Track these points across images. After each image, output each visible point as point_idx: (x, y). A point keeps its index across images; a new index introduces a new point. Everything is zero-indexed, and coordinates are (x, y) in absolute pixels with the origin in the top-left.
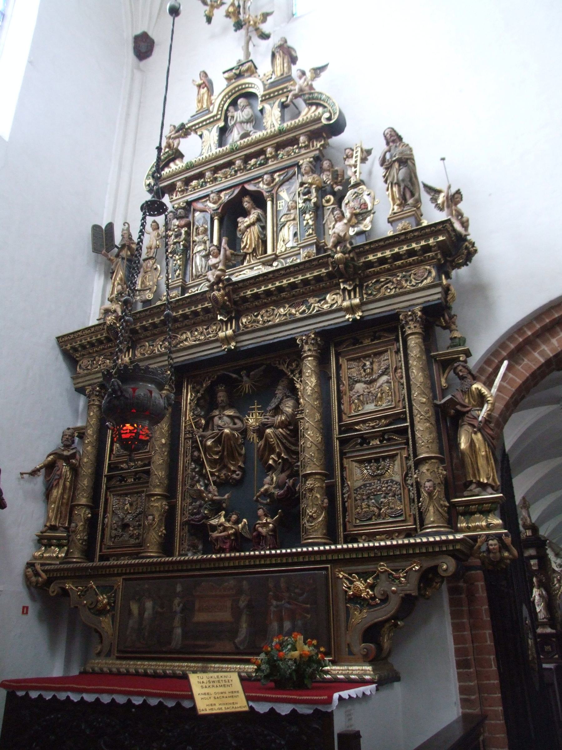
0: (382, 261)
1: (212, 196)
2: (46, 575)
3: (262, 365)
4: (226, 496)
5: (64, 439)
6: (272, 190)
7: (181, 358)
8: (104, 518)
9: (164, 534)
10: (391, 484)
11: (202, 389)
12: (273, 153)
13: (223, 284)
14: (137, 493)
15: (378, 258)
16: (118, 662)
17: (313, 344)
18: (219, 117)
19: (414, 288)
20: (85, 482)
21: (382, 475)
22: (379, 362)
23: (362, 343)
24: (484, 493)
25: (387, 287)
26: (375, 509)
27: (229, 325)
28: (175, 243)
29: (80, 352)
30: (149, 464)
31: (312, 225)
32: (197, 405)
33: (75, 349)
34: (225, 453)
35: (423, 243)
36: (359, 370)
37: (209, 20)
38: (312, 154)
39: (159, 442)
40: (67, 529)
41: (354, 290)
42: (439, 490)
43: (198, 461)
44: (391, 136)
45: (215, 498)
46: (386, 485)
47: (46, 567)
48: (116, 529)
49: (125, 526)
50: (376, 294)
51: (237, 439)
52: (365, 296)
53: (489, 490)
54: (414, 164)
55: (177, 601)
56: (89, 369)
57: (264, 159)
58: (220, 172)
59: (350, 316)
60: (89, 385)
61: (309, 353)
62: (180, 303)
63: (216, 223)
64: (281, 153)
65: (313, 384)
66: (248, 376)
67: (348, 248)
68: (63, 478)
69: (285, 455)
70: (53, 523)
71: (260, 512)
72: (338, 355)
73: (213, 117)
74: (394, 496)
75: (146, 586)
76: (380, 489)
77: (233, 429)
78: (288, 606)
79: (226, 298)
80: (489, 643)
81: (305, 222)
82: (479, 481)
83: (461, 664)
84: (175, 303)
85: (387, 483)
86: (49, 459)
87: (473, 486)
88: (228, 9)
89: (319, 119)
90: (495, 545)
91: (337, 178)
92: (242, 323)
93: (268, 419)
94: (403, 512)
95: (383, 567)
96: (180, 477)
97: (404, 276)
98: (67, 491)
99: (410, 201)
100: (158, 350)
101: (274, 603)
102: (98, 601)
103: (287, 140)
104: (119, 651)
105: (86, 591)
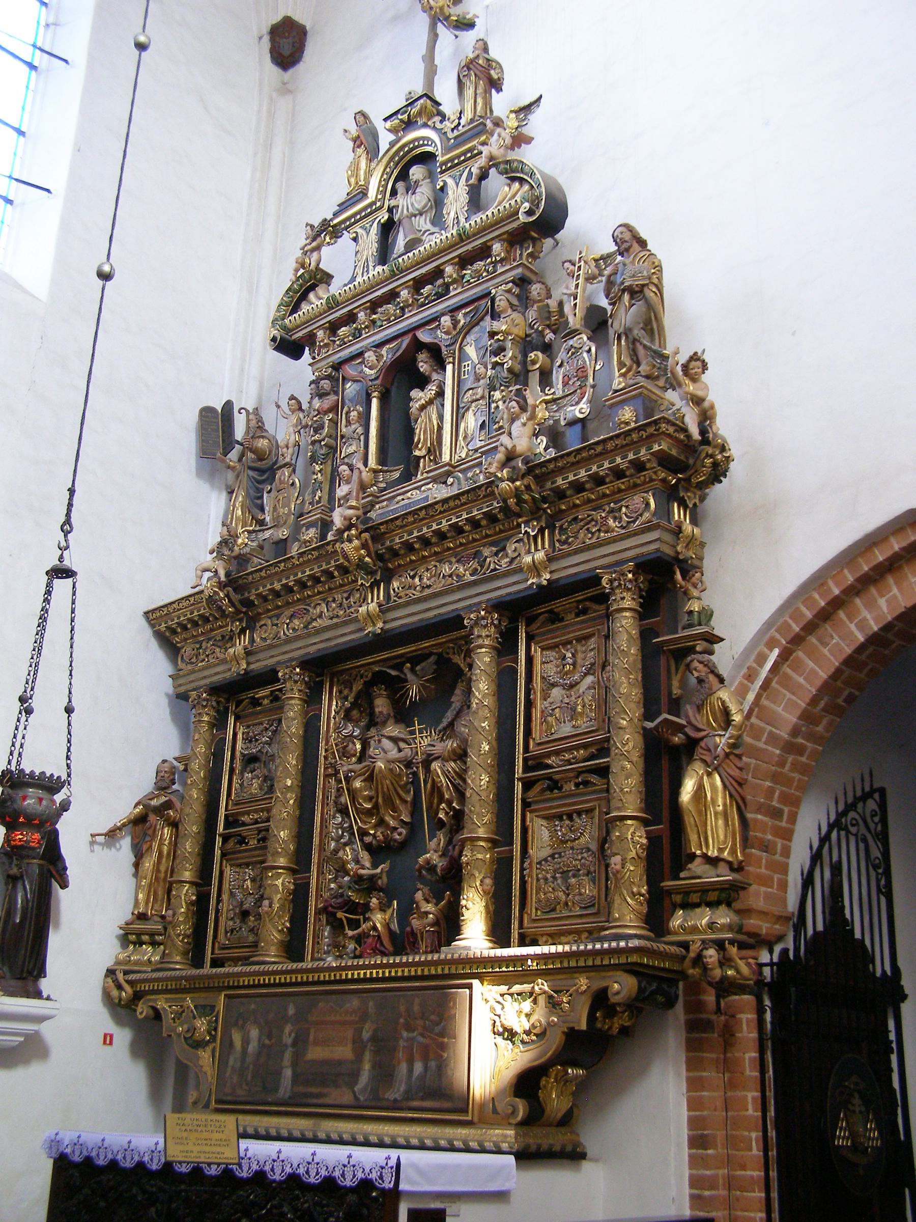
2: (132, 987)
3: (431, 654)
4: (379, 870)
6: (453, 344)
7: (314, 646)
9: (287, 928)
11: (353, 695)
12: (455, 276)
13: (357, 530)
15: (569, 483)
19: (623, 531)
20: (189, 846)
23: (562, 620)
30: (268, 820)
32: (348, 717)
33: (174, 632)
34: (380, 800)
35: (631, 456)
38: (509, 276)
41: (541, 531)
42: (632, 868)
45: (362, 872)
47: (132, 977)
48: (232, 919)
51: (400, 776)
52: (557, 545)
53: (723, 868)
55: (288, 1029)
60: (194, 690)
63: (375, 403)
66: (412, 670)
67: (520, 469)
72: (530, 638)
75: (253, 1006)
78: (421, 1039)
80: (750, 1112)
81: (493, 405)
83: (698, 1141)
87: (698, 861)
91: (549, 318)
92: (394, 590)
94: (596, 901)
96: (316, 840)
98: (164, 860)
101: (405, 1034)
103: (474, 250)
104: (218, 1101)
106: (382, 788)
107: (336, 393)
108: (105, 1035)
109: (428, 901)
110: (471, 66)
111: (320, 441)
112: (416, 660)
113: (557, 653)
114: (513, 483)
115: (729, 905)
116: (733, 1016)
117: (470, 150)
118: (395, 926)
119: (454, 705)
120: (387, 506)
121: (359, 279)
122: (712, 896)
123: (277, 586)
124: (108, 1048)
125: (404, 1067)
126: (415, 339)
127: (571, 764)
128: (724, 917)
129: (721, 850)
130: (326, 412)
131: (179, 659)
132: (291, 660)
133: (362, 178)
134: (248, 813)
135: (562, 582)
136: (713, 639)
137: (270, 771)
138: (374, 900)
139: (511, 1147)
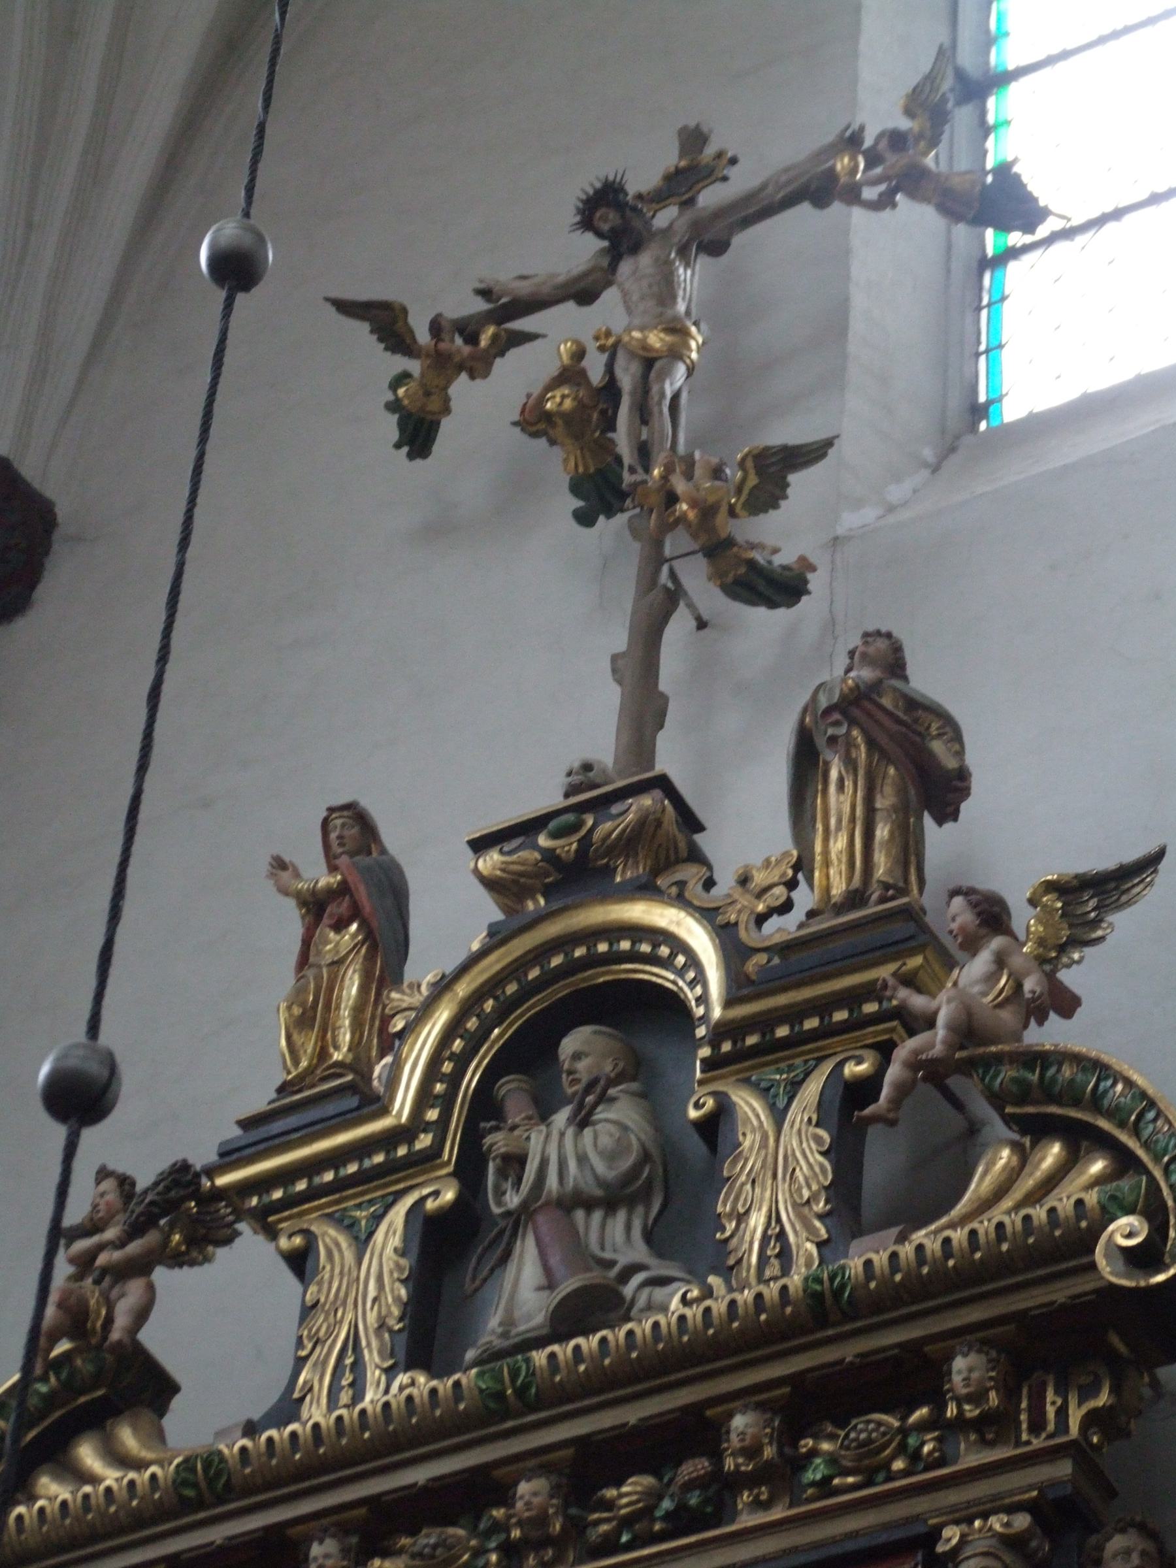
12: (769, 1452)
18: (424, 1141)
88: (542, 400)
103: (867, 1364)
110: (856, 712)
117: (852, 998)
121: (316, 1413)
133: (346, 1037)
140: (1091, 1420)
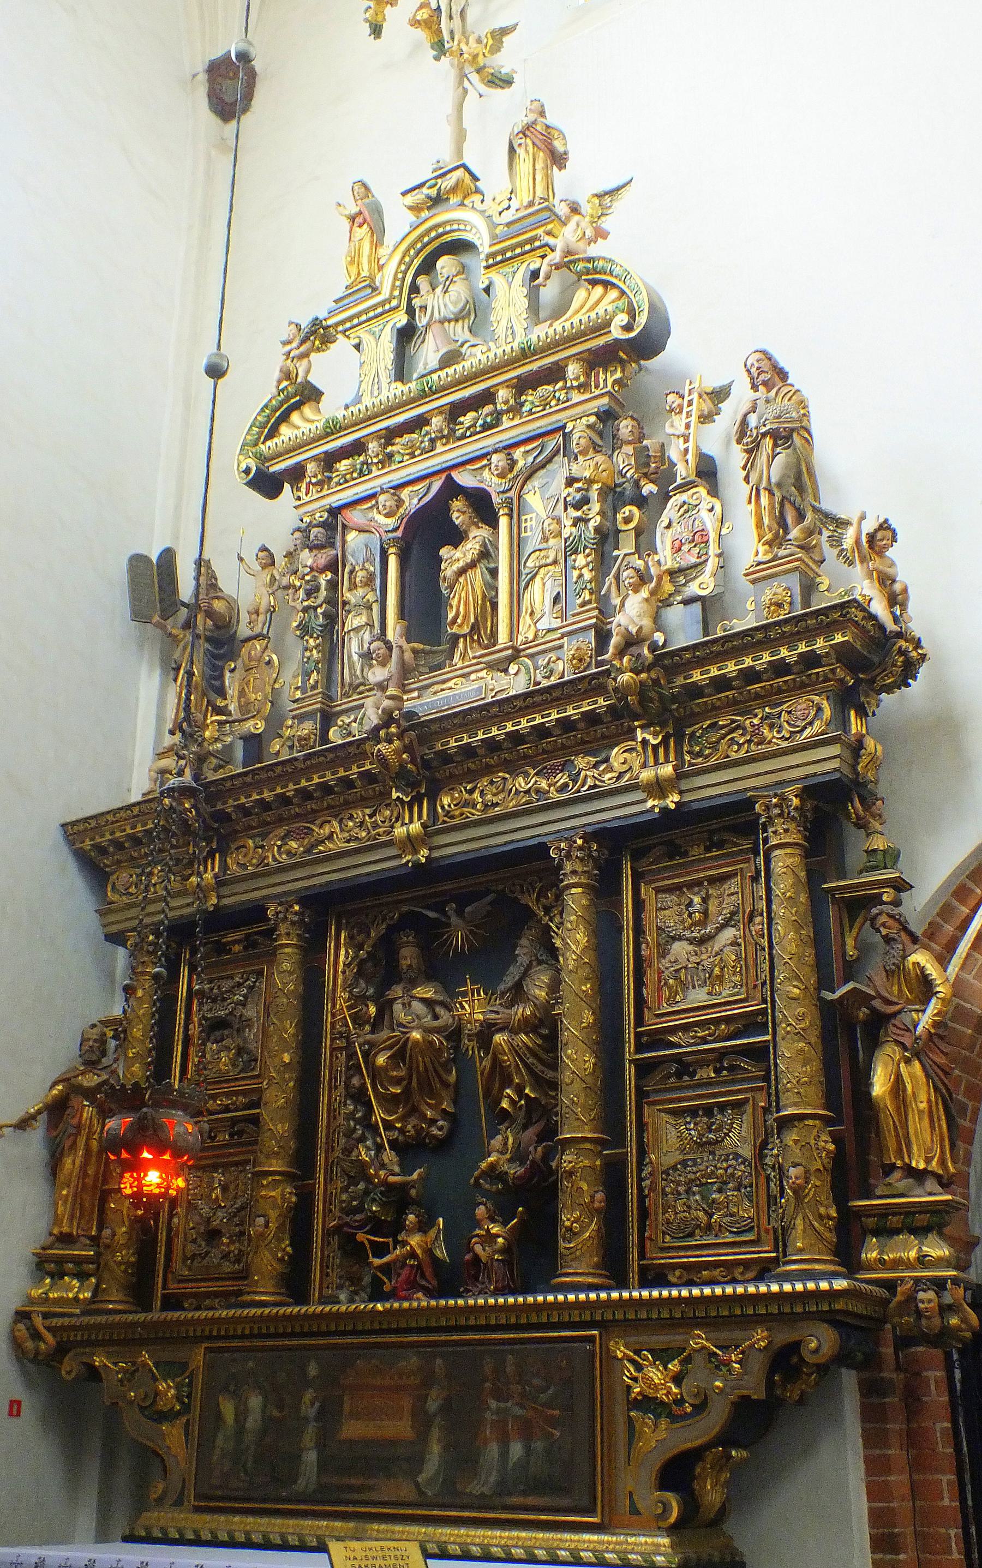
0: (721, 683)
1: (382, 498)
2: (54, 1336)
3: (488, 892)
4: (415, 1176)
5: (85, 1049)
8: (171, 1216)
9: (289, 1256)
10: (734, 1162)
11: (370, 942)
12: (512, 402)
13: (398, 727)
14: (237, 1164)
16: (197, 1517)
17: (582, 859)
21: (717, 1142)
22: (719, 896)
23: (685, 854)
24: (919, 1191)
25: (732, 739)
26: (701, 1214)
27: (416, 809)
28: (305, 610)
29: (114, 854)
31: (590, 582)
32: (360, 974)
33: (102, 851)
34: (414, 1083)
35: (802, 648)
36: (680, 914)
37: (376, 30)
38: (594, 406)
39: (277, 1061)
40: (95, 1240)
41: (665, 741)
42: (818, 1183)
43: (359, 1096)
44: (761, 371)
45: (392, 1179)
46: (725, 1165)
47: (55, 1322)
48: (194, 1241)
49: (213, 1235)
50: (711, 754)
51: (439, 1051)
52: (687, 758)
53: (931, 1184)
54: (808, 442)
55: (308, 1396)
56: (132, 894)
57: (491, 414)
58: (398, 440)
59: (656, 803)
61: (575, 880)
62: (315, 761)
63: (393, 562)
64: (530, 398)
65: (581, 946)
66: (460, 912)
67: (647, 658)
68: (84, 1133)
69: (531, 1090)
70: (65, 1229)
71: (481, 1211)
72: (638, 878)
73: (383, 303)
74: (738, 1189)
76: (713, 1172)
77: (427, 1031)
78: (519, 1412)
79: (404, 756)
81: (576, 573)
82: (909, 1166)
84: (304, 761)
85: (726, 1160)
86: (55, 1092)
87: (897, 1175)
89: (604, 326)
90: (930, 1301)
91: (647, 465)
92: (442, 807)
93: (497, 1013)
94: (755, 1224)
95: (699, 1340)
96: (322, 1134)
97: (767, 717)
98: (94, 1159)
99: (795, 533)
100: (275, 859)
101: (494, 1404)
102: (157, 1393)
104: (198, 1497)
105: (133, 1374)
106: (418, 1066)
107: (332, 545)
108: (12, 1402)
109: (493, 1220)
110: (527, 133)
111: (315, 608)
112: (463, 900)
113: (678, 896)
114: (637, 675)
115: (941, 1234)
116: (917, 1374)
117: (531, 241)
118: (441, 1253)
119: (519, 959)
120: (419, 697)
122: (921, 1220)
123: (268, 795)
124: (15, 1420)
125: (493, 1450)
126: (450, 482)
127: (706, 1043)
128: (937, 1250)
129: (928, 1161)
130: (322, 571)
131: (109, 889)
132: (285, 894)
134: (214, 1097)
135: (696, 806)
136: (901, 886)
137: (245, 1040)
138: (411, 1217)
139: (669, 1562)
140: (616, 382)
